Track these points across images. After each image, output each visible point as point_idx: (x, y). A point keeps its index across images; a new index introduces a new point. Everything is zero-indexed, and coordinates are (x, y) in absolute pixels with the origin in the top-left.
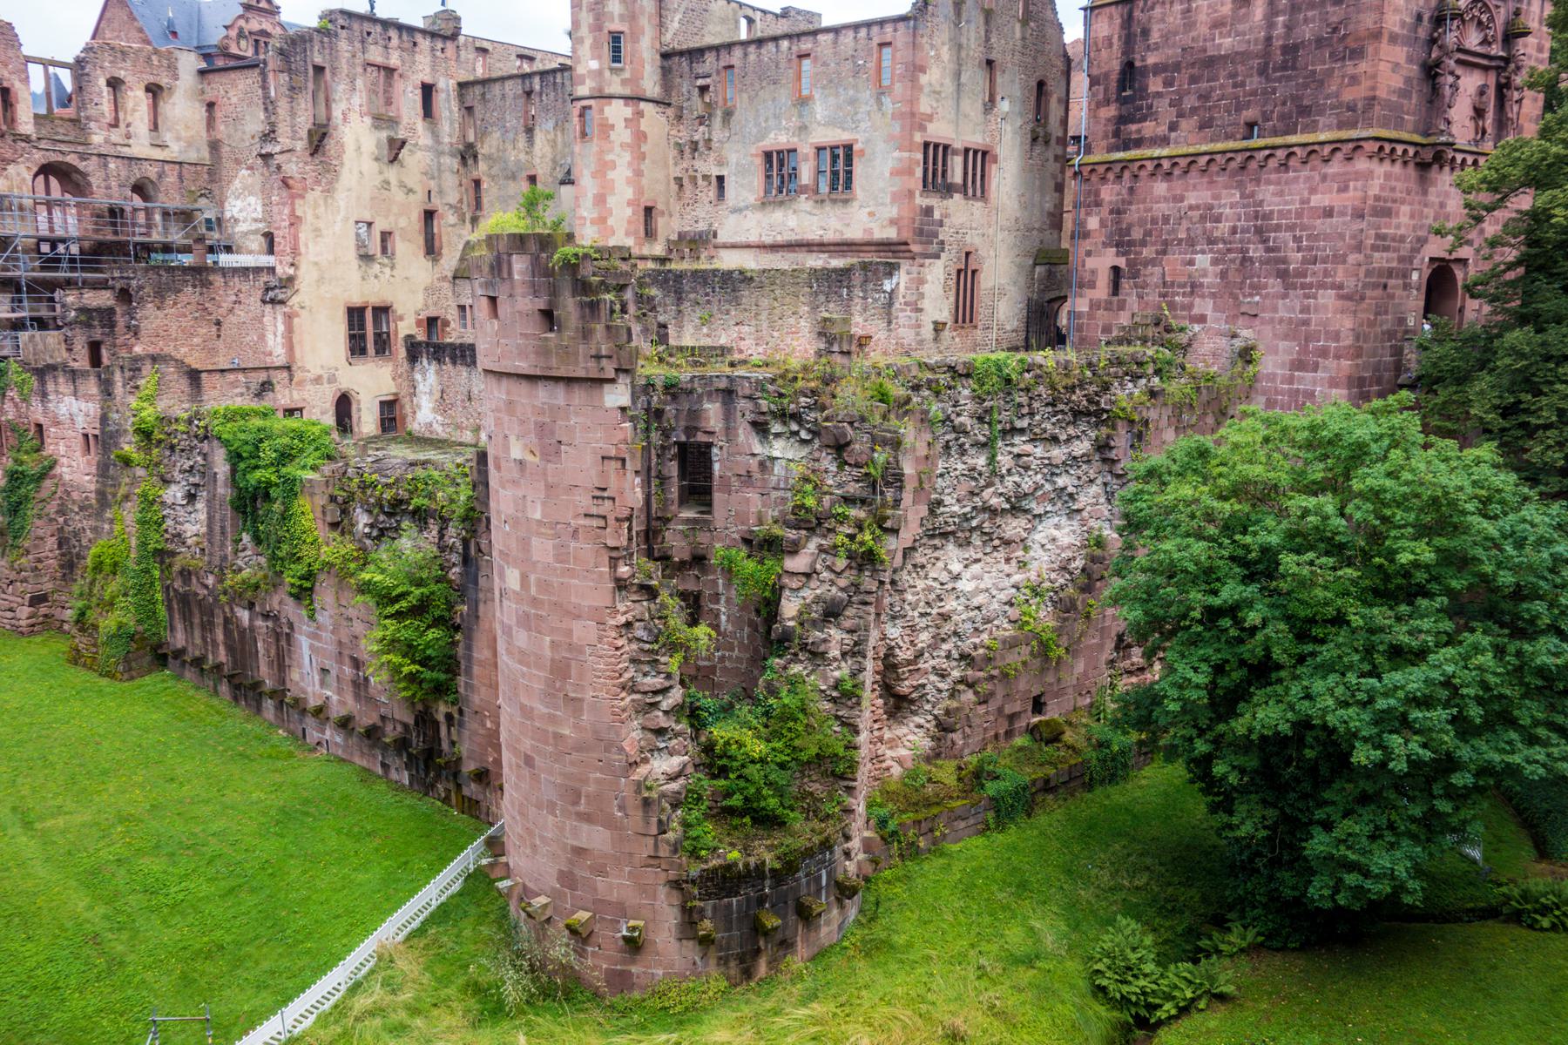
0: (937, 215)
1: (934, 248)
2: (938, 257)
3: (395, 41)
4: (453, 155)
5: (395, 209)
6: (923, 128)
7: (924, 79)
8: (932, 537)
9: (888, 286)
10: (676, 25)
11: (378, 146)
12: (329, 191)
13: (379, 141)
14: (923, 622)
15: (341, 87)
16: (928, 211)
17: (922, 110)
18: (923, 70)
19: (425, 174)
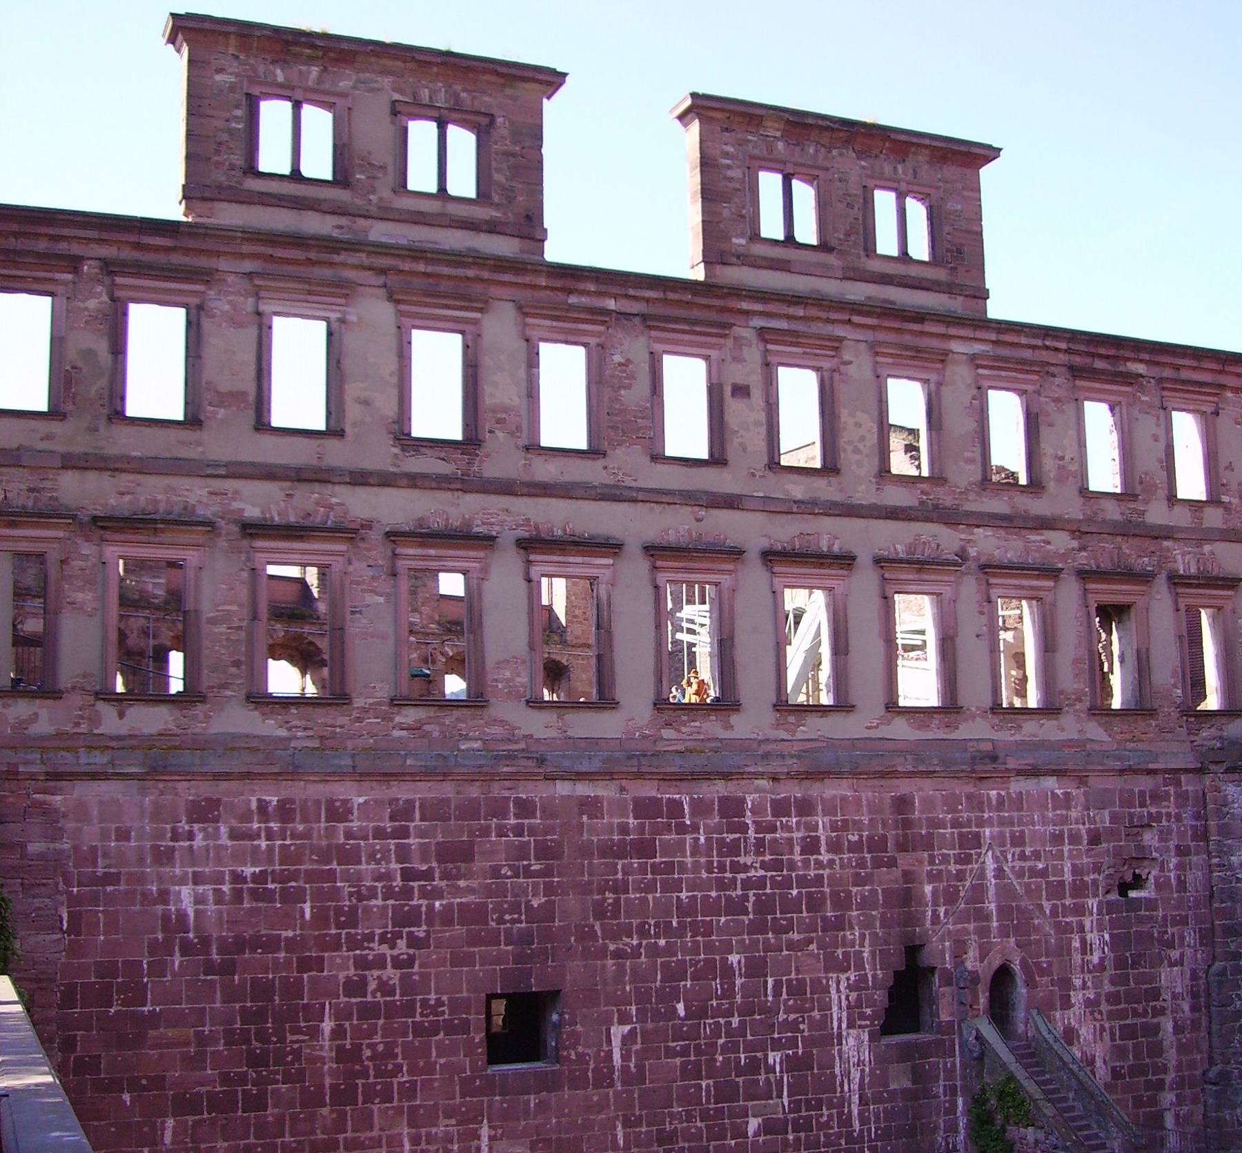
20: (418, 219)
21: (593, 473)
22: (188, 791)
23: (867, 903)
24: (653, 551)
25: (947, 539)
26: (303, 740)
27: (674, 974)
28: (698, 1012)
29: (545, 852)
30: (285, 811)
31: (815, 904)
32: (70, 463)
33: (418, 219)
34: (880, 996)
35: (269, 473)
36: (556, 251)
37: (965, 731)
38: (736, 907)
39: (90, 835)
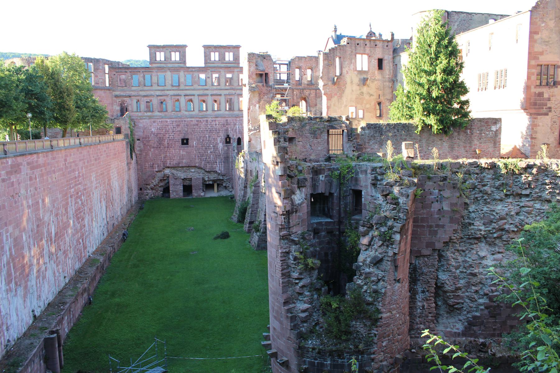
0: (546, 96)
1: (544, 110)
2: (547, 114)
3: (368, 45)
4: (390, 82)
5: (365, 102)
6: (536, 58)
7: (536, 37)
8: (469, 239)
9: (494, 128)
10: (456, 27)
11: (359, 81)
12: (340, 97)
13: (360, 79)
14: (462, 276)
15: (346, 63)
16: (541, 94)
17: (536, 50)
18: (537, 33)
19: (378, 89)
20: (173, 63)
21: (192, 88)
22: (153, 120)
23: (222, 130)
24: (198, 95)
25: (233, 92)
26: (163, 115)
27: (200, 137)
28: (203, 141)
29: (187, 125)
30: (162, 122)
31: (216, 130)
32: (141, 91)
33: (173, 63)
34: (224, 140)
35: (159, 90)
36: (188, 65)
37: (235, 113)
38: (207, 131)
39: (144, 124)
